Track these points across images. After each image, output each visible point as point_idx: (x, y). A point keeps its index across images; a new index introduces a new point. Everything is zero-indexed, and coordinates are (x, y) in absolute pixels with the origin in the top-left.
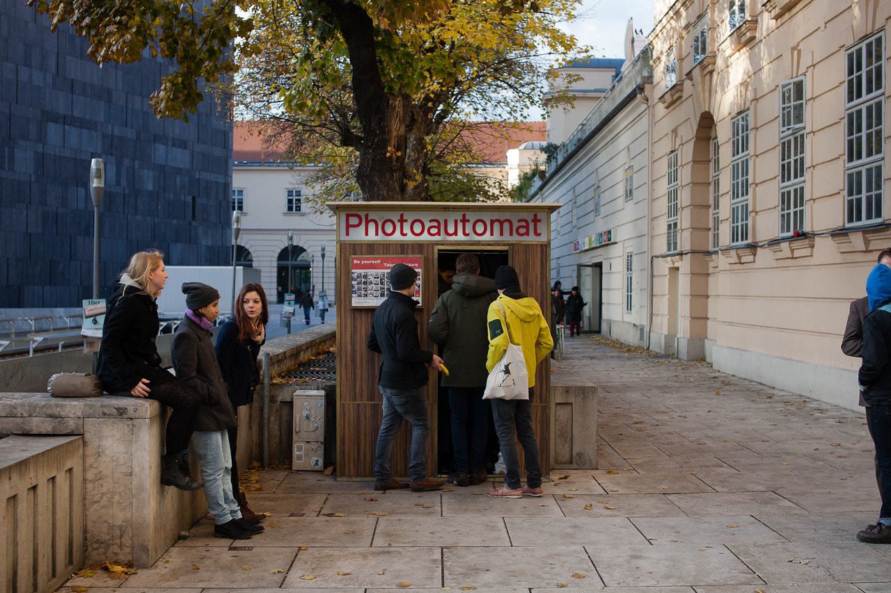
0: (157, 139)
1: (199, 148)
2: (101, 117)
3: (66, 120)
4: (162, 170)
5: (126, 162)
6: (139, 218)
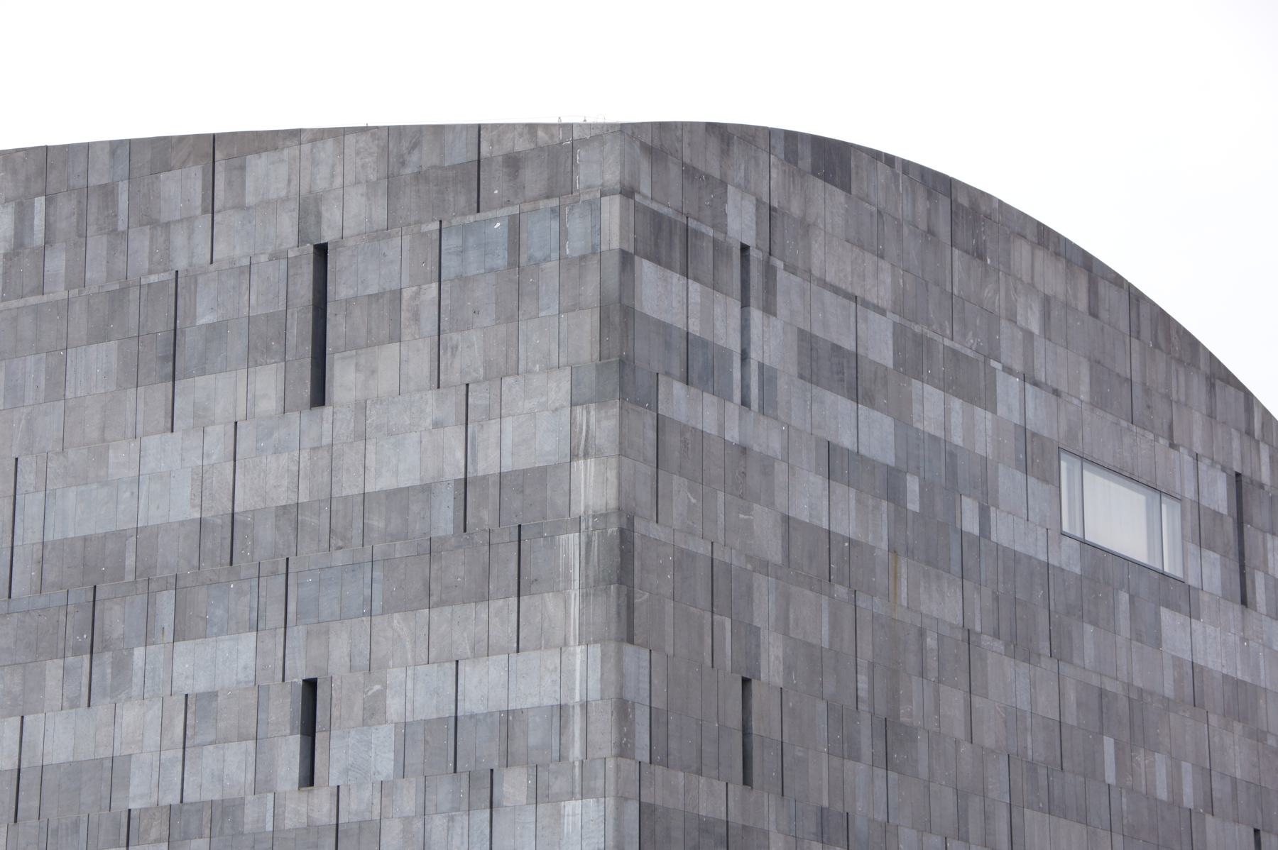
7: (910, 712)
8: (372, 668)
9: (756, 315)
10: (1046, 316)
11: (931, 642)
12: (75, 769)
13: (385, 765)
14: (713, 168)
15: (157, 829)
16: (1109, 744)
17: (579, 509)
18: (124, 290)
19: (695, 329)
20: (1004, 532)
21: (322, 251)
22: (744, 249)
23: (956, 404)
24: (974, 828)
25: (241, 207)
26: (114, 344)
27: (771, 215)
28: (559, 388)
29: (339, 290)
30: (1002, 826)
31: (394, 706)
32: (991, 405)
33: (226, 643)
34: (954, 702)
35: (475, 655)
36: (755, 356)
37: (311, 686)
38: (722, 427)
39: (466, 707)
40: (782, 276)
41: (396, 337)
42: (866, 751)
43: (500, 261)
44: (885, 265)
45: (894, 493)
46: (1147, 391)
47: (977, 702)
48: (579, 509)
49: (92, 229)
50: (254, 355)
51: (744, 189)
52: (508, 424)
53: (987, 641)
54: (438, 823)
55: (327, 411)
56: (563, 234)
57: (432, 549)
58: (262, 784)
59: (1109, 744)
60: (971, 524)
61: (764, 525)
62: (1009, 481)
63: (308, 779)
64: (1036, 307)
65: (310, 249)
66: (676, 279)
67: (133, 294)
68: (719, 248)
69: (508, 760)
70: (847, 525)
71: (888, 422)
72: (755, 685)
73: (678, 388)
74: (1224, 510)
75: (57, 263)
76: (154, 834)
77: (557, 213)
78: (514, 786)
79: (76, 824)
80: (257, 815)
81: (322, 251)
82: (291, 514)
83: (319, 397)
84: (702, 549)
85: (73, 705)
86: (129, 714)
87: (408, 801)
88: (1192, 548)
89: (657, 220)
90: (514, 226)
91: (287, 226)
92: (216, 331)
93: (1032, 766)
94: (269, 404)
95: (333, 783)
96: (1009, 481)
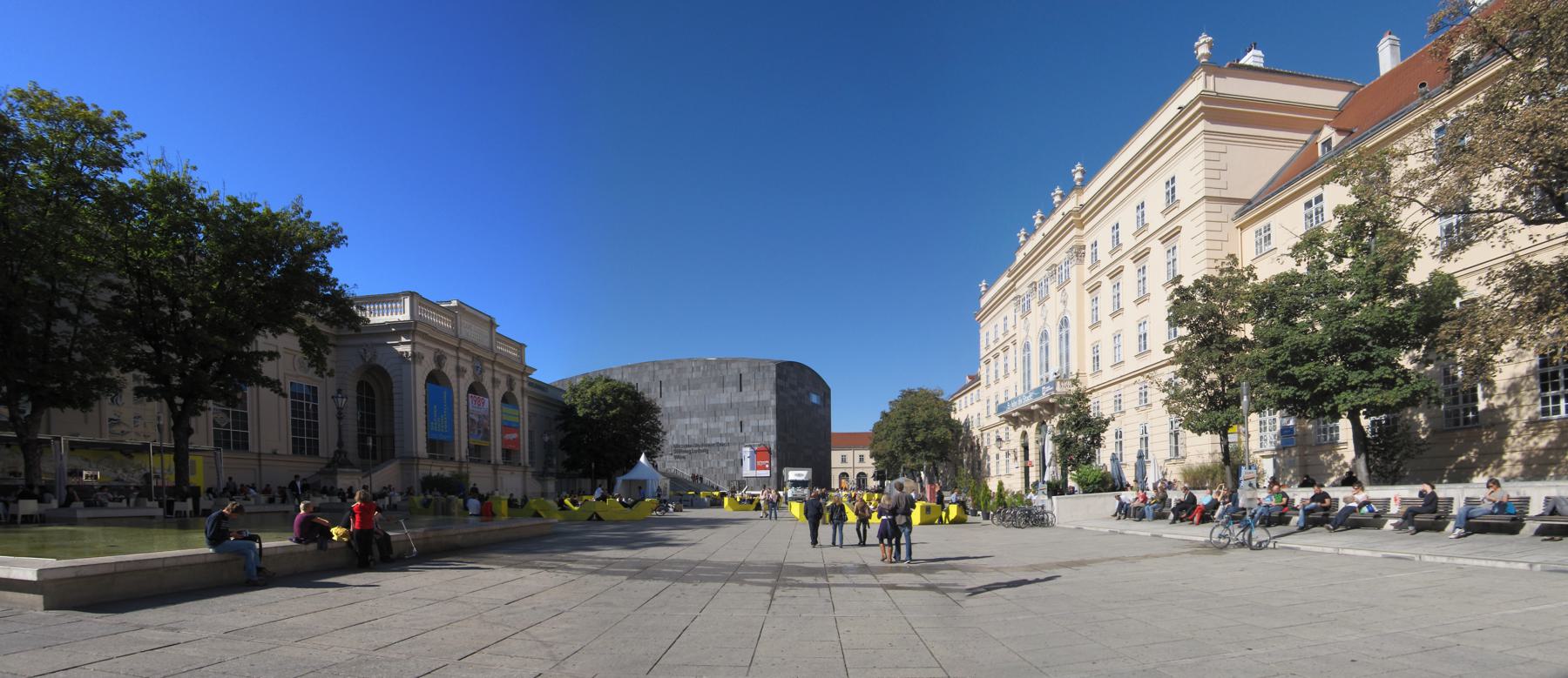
8: (748, 420)
12: (714, 429)
13: (750, 430)
21: (741, 375)
29: (743, 379)
31: (751, 425)
37: (741, 422)
50: (733, 385)
57: (755, 408)
58: (736, 431)
75: (709, 373)
78: (765, 433)
81: (741, 375)
82: (738, 404)
83: (741, 390)
86: (720, 424)
87: (753, 434)
90: (764, 374)
91: (736, 371)
92: (728, 383)
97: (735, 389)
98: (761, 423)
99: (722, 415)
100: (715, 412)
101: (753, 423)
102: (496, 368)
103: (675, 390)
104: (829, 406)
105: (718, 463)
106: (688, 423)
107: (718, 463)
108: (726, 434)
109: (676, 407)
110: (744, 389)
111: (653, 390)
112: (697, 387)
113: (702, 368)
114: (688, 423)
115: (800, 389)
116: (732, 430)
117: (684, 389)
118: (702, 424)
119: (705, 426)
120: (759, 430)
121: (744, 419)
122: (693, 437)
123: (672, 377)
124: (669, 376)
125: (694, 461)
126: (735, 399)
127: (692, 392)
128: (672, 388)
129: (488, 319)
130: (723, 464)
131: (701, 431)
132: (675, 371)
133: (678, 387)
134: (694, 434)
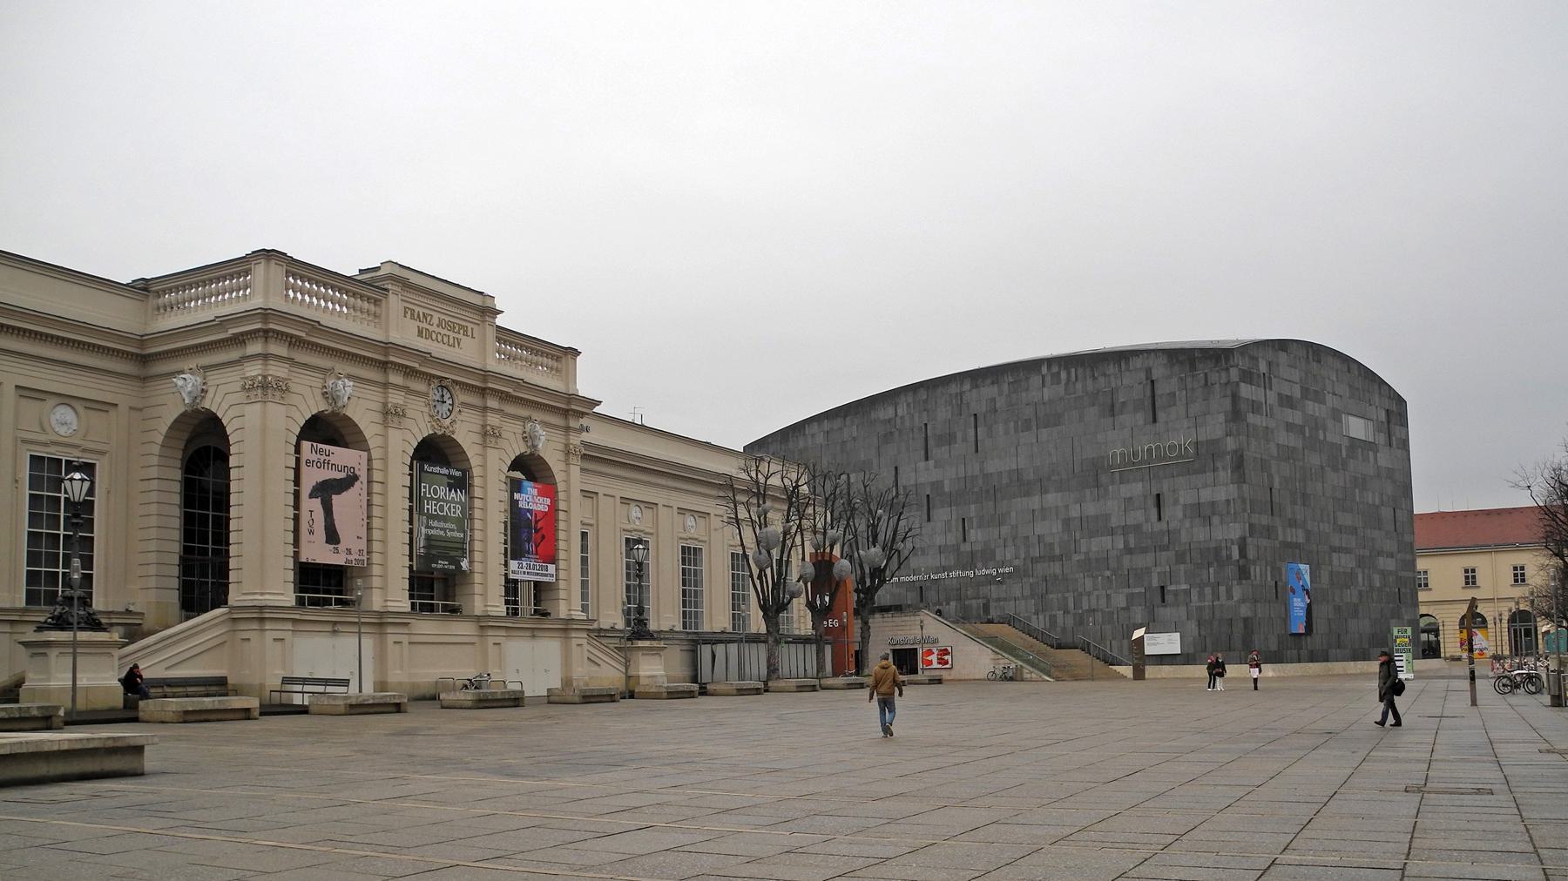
0: (1380, 553)
1: (1399, 556)
2: (1354, 545)
3: (1339, 550)
4: (1384, 574)
5: (1366, 571)
6: (1374, 605)
7: (1309, 491)
9: (1268, 391)
10: (1337, 378)
11: (1313, 471)
13: (1180, 515)
14: (1256, 355)
15: (1120, 532)
16: (1357, 490)
17: (1229, 449)
18: (1098, 393)
19: (1254, 398)
20: (1329, 438)
22: (1264, 374)
23: (1316, 405)
24: (1325, 519)
25: (1129, 370)
26: (1096, 407)
27: (1270, 364)
28: (1221, 418)
29: (1158, 392)
30: (1332, 517)
31: (1182, 501)
32: (1325, 404)
33: (1134, 484)
34: (1320, 484)
35: (1203, 488)
36: (1268, 402)
37: (1158, 495)
38: (1262, 422)
39: (1201, 501)
40: (1274, 380)
41: (1175, 405)
42: (1299, 503)
43: (1203, 382)
44: (1297, 371)
45: (1304, 434)
46: (1364, 391)
47: (1325, 485)
48: (1229, 449)
49: (1088, 378)
51: (1263, 358)
52: (1208, 428)
53: (1326, 468)
54: (1195, 530)
55: (1157, 424)
56: (1220, 377)
58: (1147, 521)
59: (1357, 490)
60: (1321, 437)
61: (1273, 447)
62: (1330, 424)
63: (1160, 519)
64: (1335, 373)
65: (1149, 381)
66: (1249, 386)
67: (1100, 393)
68: (1259, 375)
69: (1214, 514)
70: (1292, 444)
71: (1300, 413)
72: (1273, 490)
73: (1251, 415)
74: (1384, 420)
75: (1079, 386)
76: (1119, 533)
77: (1218, 371)
78: (1216, 520)
79: (1098, 531)
80: (1147, 528)
81: (1153, 382)
83: (1155, 421)
84: (1259, 456)
85: (1094, 501)
86: (1109, 503)
87: (1187, 524)
88: (1376, 433)
89: (1244, 371)
90: (1206, 374)
91: (1143, 375)
93: (1339, 500)
94: (1141, 422)
95: (1167, 520)
96: (1330, 424)
97: (1140, 418)
98: (1206, 495)
99: (1113, 483)
100: (1095, 475)
101: (1186, 497)
102: (492, 403)
103: (1007, 433)
104: (1405, 444)
105: (1108, 596)
106: (1037, 506)
107: (1108, 596)
108: (1125, 530)
109: (1010, 472)
110: (1161, 416)
111: (959, 435)
112: (1054, 420)
113: (1063, 375)
114: (1037, 506)
115: (1312, 407)
116: (1136, 517)
117: (1027, 428)
118: (1067, 507)
119: (1075, 512)
120: (1202, 513)
121: (1165, 487)
122: (1048, 540)
123: (1001, 403)
124: (993, 400)
125: (1051, 596)
126: (1144, 444)
127: (1044, 433)
128: (1001, 428)
129: (477, 300)
130: (1120, 600)
131: (1067, 522)
132: (1006, 386)
133: (1012, 424)
134: (1051, 529)
